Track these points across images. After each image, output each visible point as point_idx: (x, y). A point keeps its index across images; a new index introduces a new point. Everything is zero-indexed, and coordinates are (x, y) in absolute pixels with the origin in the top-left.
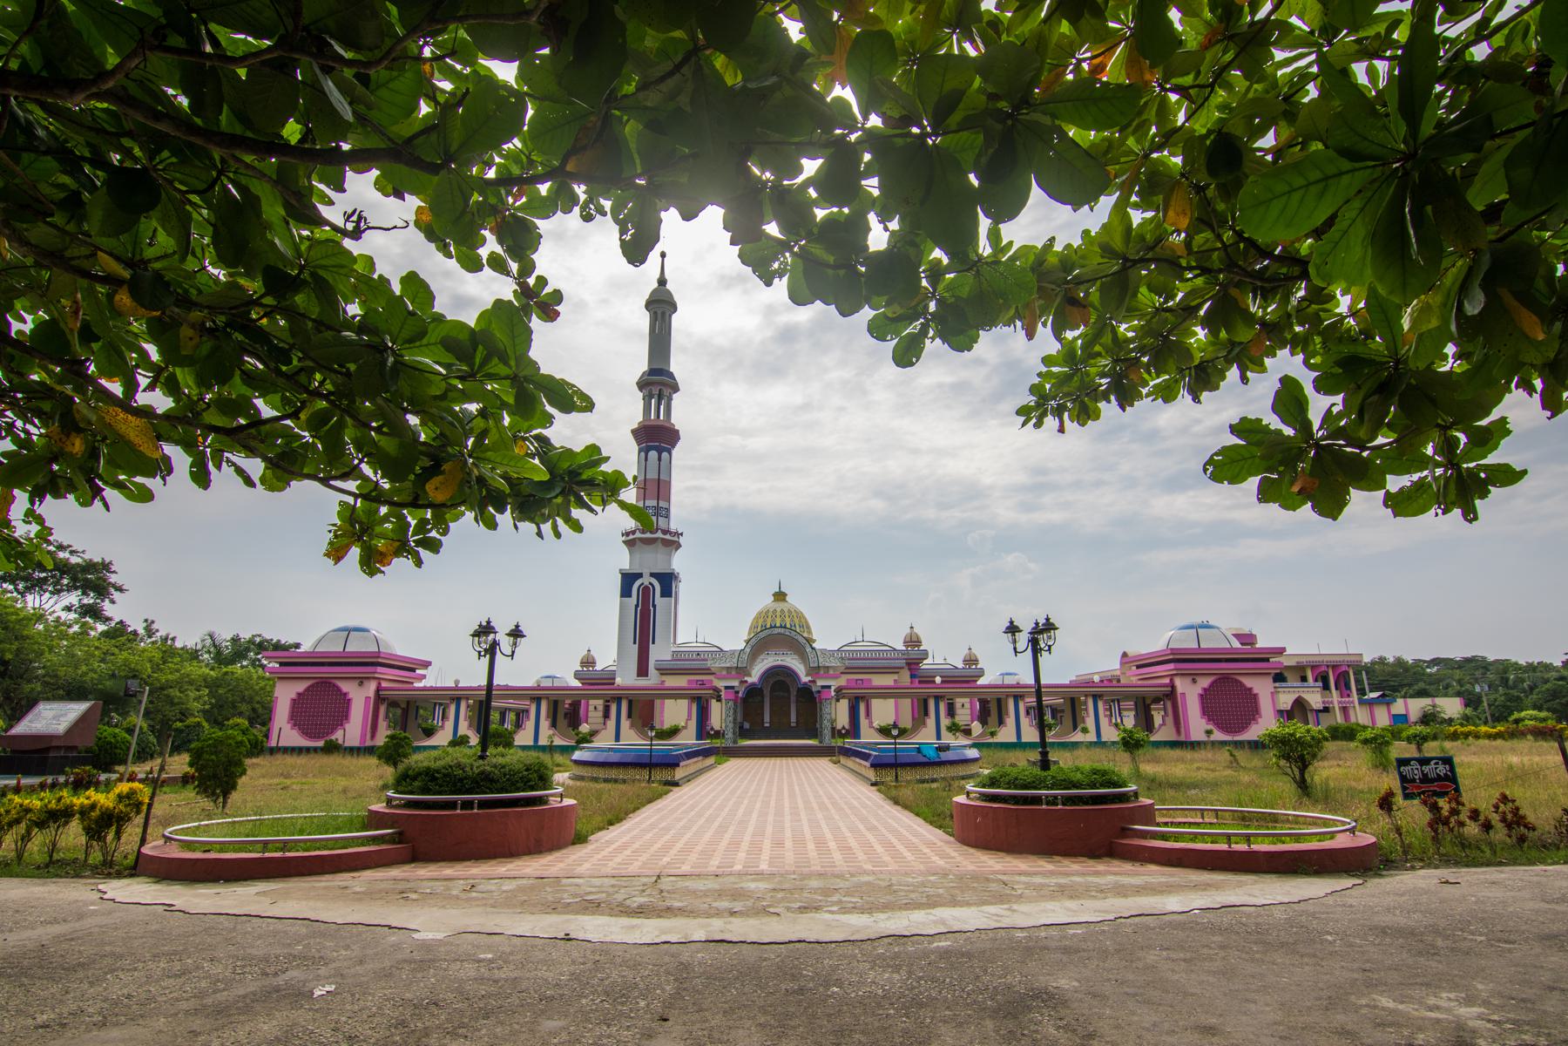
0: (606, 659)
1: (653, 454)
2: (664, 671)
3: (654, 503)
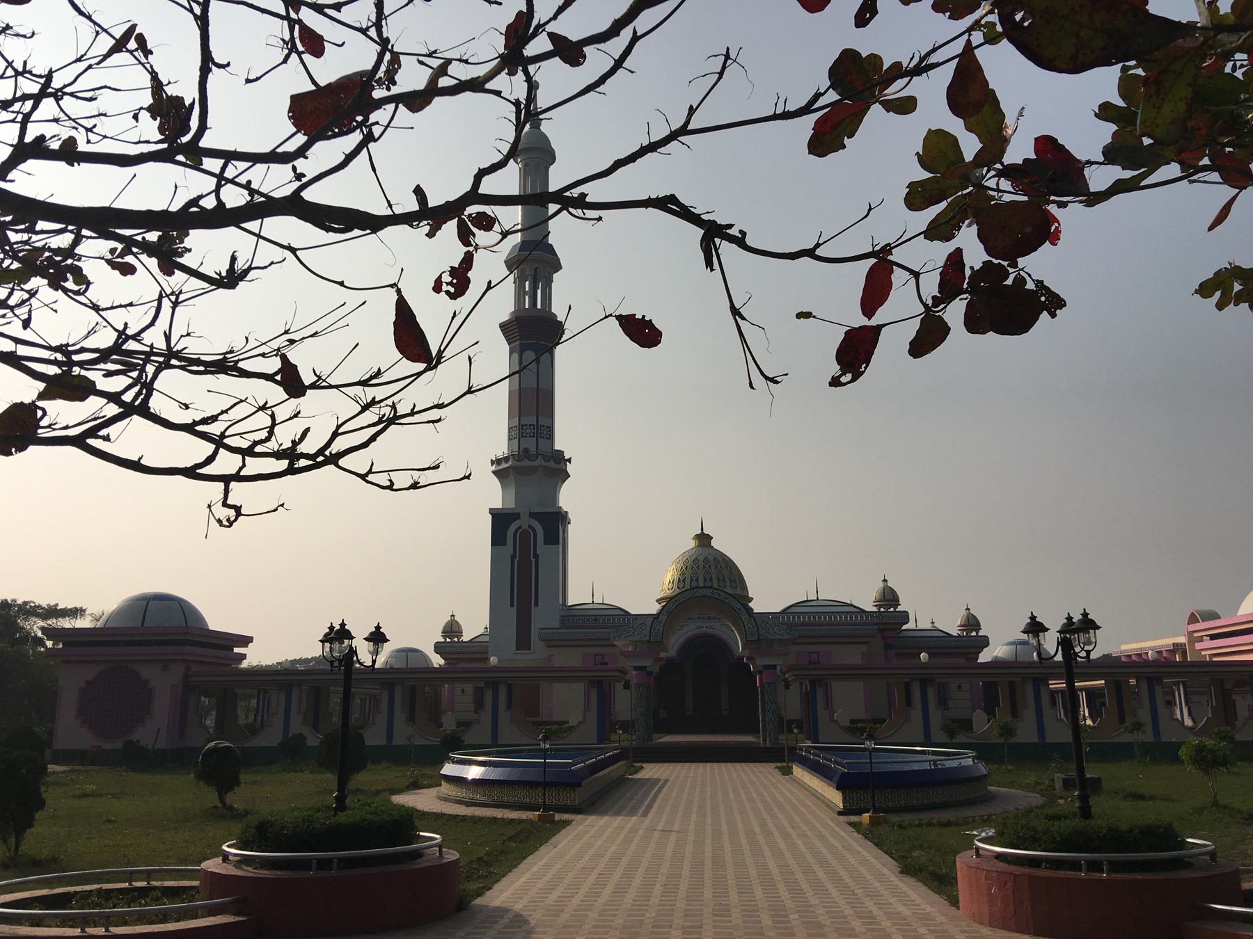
0: (475, 624)
1: (530, 355)
2: (551, 641)
3: (532, 420)
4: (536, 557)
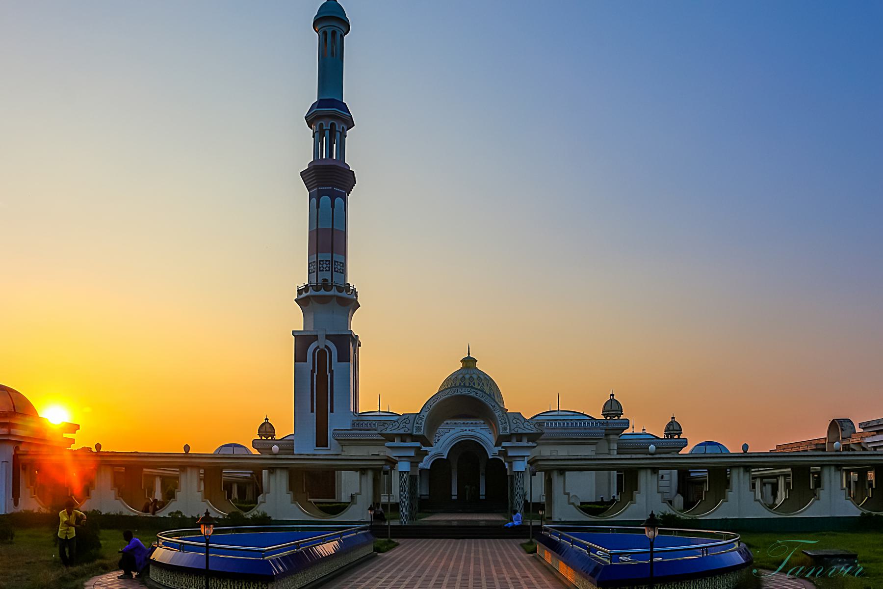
2: (344, 442)
4: (331, 372)
